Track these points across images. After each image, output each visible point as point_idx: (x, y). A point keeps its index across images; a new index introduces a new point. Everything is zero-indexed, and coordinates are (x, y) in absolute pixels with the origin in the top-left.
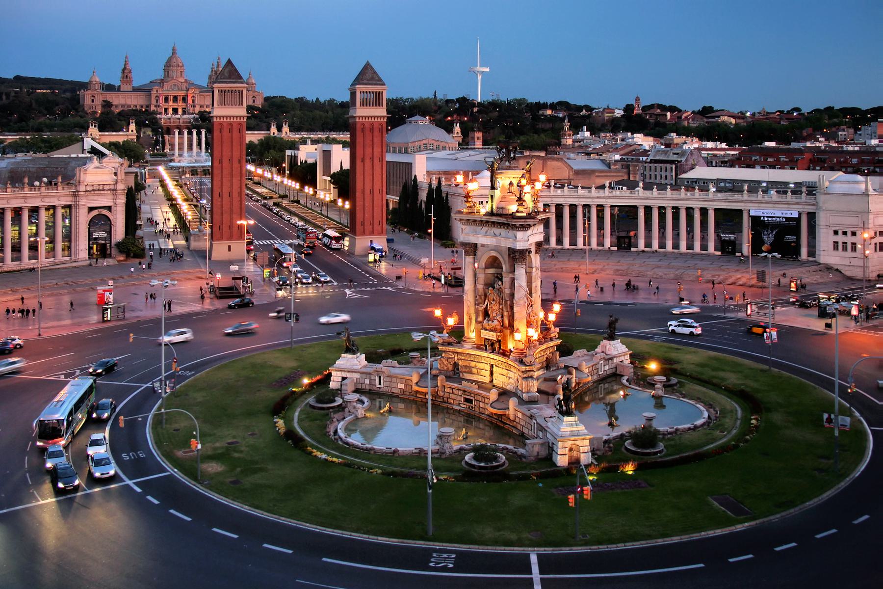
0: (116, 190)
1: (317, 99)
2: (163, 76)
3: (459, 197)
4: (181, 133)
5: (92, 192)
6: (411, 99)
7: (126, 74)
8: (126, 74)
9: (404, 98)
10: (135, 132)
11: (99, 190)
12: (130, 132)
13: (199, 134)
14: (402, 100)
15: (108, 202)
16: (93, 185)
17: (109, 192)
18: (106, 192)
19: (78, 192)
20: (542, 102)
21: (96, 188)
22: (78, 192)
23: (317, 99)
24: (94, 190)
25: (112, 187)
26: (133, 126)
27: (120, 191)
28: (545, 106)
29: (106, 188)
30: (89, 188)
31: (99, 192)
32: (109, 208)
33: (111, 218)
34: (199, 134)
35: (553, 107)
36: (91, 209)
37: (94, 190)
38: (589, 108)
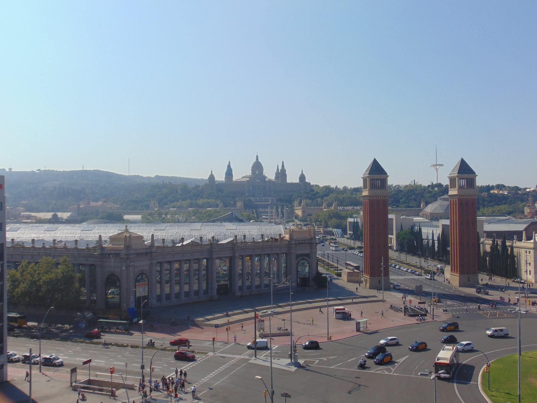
0: (312, 244)
1: (336, 186)
2: (251, 174)
3: (523, 249)
4: (272, 208)
5: (299, 245)
6: (398, 185)
7: (229, 173)
8: (229, 173)
9: (394, 185)
10: (243, 207)
11: (302, 243)
12: (238, 208)
13: (282, 208)
14: (392, 186)
15: (307, 251)
16: (299, 240)
17: (308, 245)
18: (306, 245)
19: (291, 244)
20: (491, 185)
21: (301, 242)
22: (291, 244)
23: (336, 186)
24: (299, 243)
25: (309, 241)
26: (239, 204)
27: (314, 244)
28: (493, 188)
29: (306, 242)
30: (297, 242)
31: (303, 245)
32: (308, 255)
33: (309, 261)
34: (282, 208)
35: (500, 187)
36: (298, 256)
37: (299, 243)
38: (517, 188)
